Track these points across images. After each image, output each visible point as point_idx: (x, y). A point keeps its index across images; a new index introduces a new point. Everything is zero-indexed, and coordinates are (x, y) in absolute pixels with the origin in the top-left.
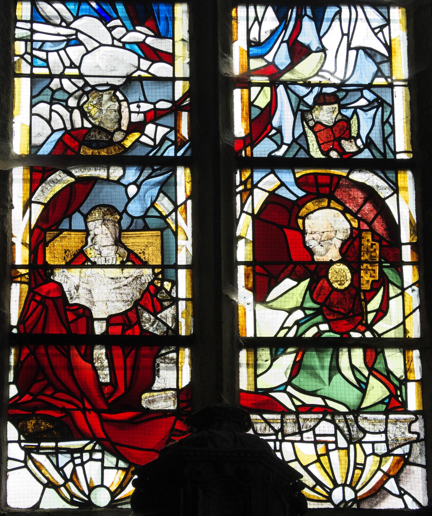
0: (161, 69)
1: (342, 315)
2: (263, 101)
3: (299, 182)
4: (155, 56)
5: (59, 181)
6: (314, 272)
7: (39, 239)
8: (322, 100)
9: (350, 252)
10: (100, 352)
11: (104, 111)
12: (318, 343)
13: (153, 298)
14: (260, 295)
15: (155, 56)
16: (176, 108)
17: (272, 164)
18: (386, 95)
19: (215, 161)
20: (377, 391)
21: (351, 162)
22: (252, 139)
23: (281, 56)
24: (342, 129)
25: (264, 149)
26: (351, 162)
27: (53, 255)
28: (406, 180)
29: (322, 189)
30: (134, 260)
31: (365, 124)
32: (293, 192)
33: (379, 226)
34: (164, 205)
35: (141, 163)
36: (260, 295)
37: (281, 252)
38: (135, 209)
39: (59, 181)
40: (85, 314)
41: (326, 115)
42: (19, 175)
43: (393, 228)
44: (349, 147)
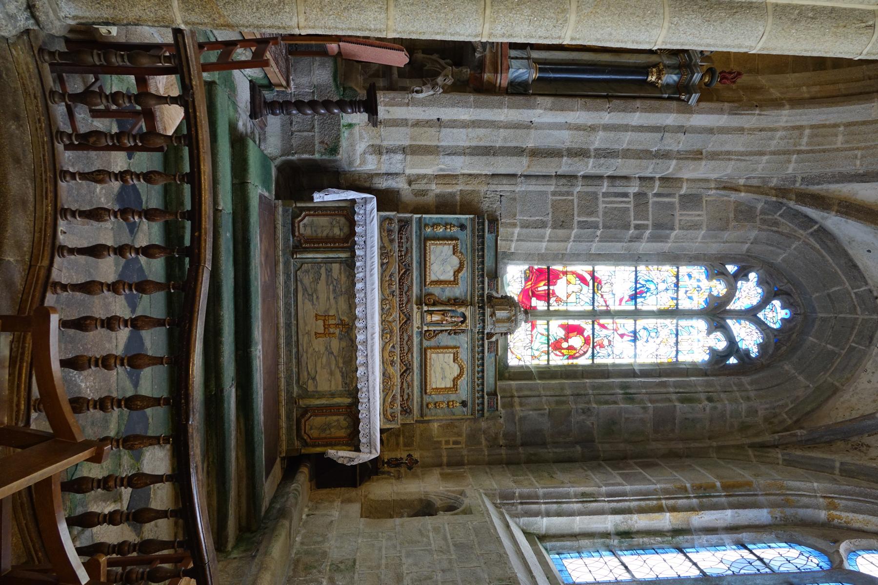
0: (617, 302)
1: (557, 346)
2: (609, 327)
3: (588, 336)
4: (621, 300)
5: (588, 278)
6: (566, 339)
7: (573, 273)
8: (610, 341)
9: (571, 348)
10: (546, 288)
11: (606, 288)
12: (548, 340)
13: (558, 300)
14: (562, 326)
15: (621, 300)
16: (607, 306)
17: (593, 329)
18: (611, 357)
19: (594, 315)
20: (537, 353)
21: (594, 347)
22: (599, 324)
23: (620, 332)
24: (602, 346)
25: (596, 326)
26: (594, 347)
27: (571, 277)
28: (590, 362)
29: (587, 341)
30: (568, 296)
31: (603, 352)
32: (586, 334)
33: (577, 355)
34: (582, 303)
35: (593, 298)
36: (562, 326)
37: (571, 330)
38: (581, 296)
39: (588, 278)
40: (555, 284)
41: (606, 343)
42: (590, 268)
43: (577, 358)
44: (598, 347)
